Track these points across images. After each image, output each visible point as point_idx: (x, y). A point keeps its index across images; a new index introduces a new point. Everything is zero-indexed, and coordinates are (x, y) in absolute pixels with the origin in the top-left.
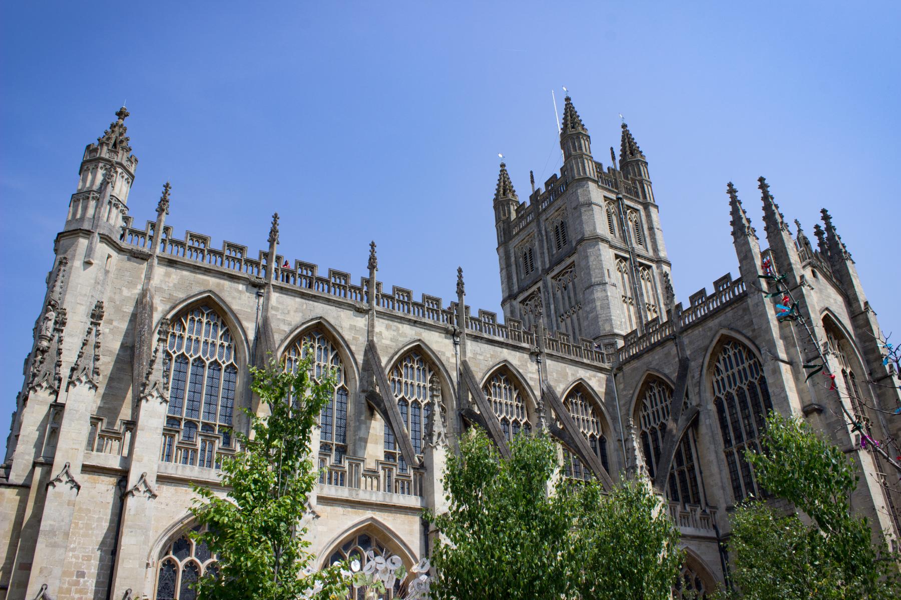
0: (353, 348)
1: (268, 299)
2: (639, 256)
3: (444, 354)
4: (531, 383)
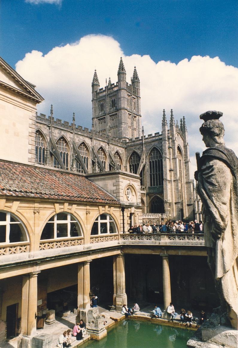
0: (70, 143)
1: (52, 130)
2: (134, 114)
3: (89, 144)
4: (107, 151)
